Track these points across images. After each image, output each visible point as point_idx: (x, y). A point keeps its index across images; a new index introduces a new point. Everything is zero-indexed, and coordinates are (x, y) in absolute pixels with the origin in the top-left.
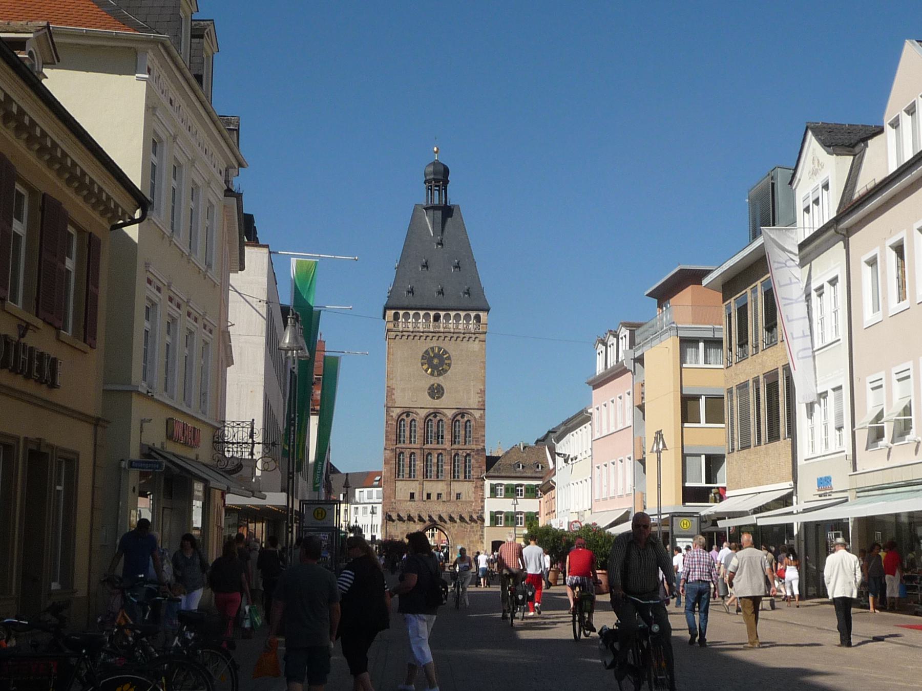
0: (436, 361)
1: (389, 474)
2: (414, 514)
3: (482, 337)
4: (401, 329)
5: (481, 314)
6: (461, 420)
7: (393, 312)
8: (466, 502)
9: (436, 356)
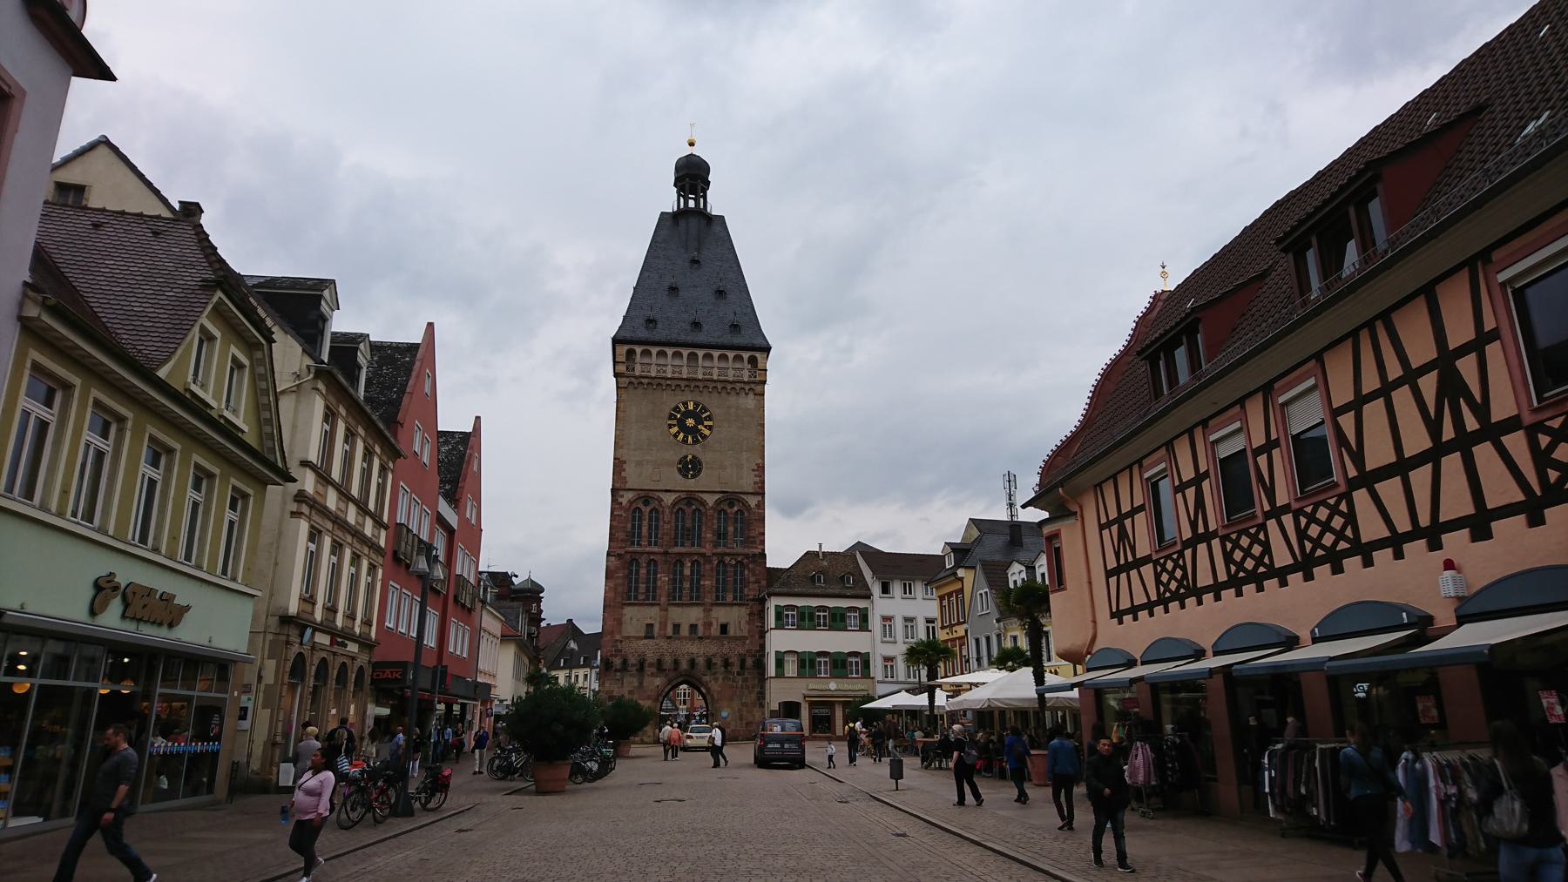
0: (690, 422)
1: (612, 595)
2: (651, 657)
3: (758, 389)
4: (637, 373)
5: (758, 355)
7: (626, 347)
8: (736, 638)
9: (688, 414)
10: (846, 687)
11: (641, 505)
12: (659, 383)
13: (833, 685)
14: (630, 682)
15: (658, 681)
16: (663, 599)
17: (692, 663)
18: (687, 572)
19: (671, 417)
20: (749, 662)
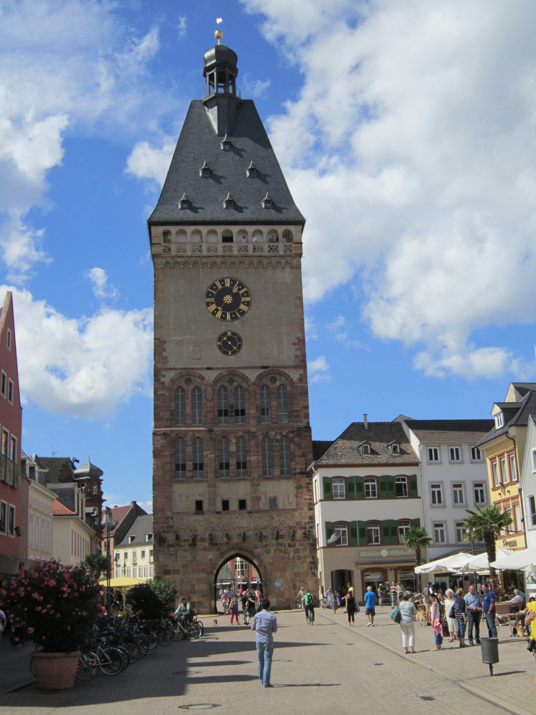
0: (228, 299)
2: (202, 533)
3: (295, 262)
5: (292, 228)
6: (271, 386)
7: (162, 229)
10: (397, 553)
11: (184, 386)
12: (195, 262)
13: (384, 552)
14: (184, 555)
15: (211, 555)
16: (211, 476)
17: (244, 537)
18: (233, 448)
19: (208, 295)
20: (299, 534)
